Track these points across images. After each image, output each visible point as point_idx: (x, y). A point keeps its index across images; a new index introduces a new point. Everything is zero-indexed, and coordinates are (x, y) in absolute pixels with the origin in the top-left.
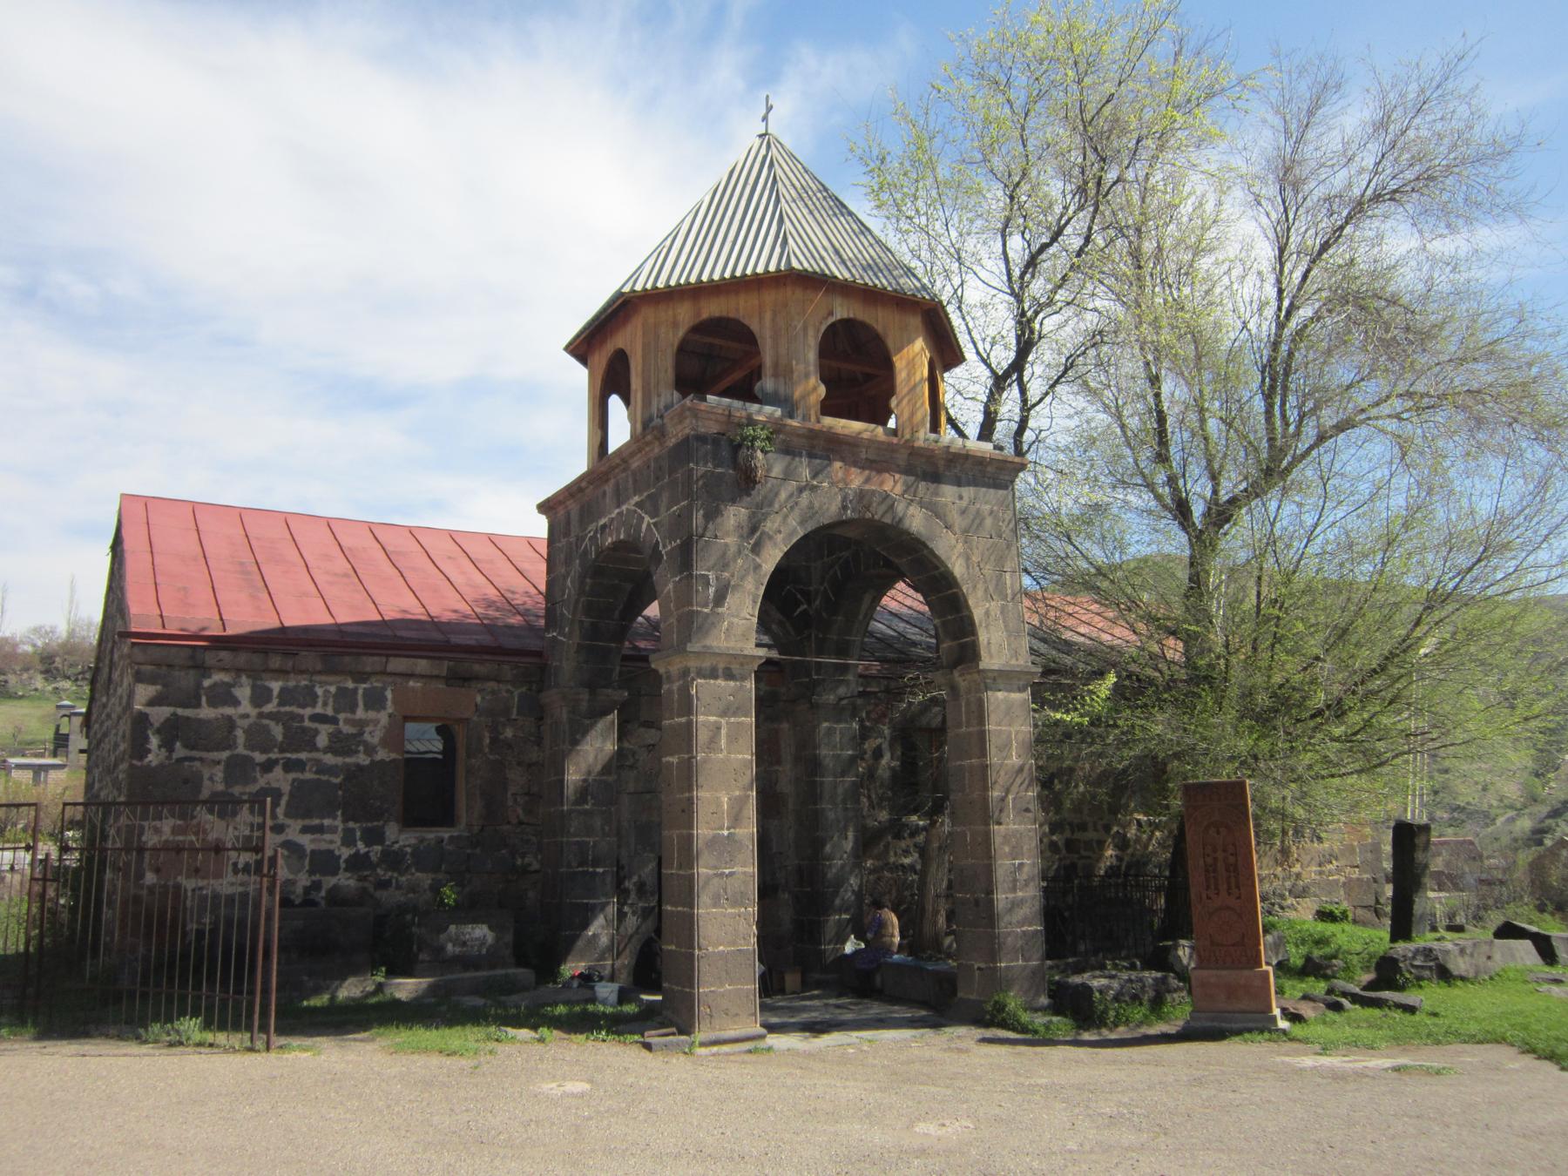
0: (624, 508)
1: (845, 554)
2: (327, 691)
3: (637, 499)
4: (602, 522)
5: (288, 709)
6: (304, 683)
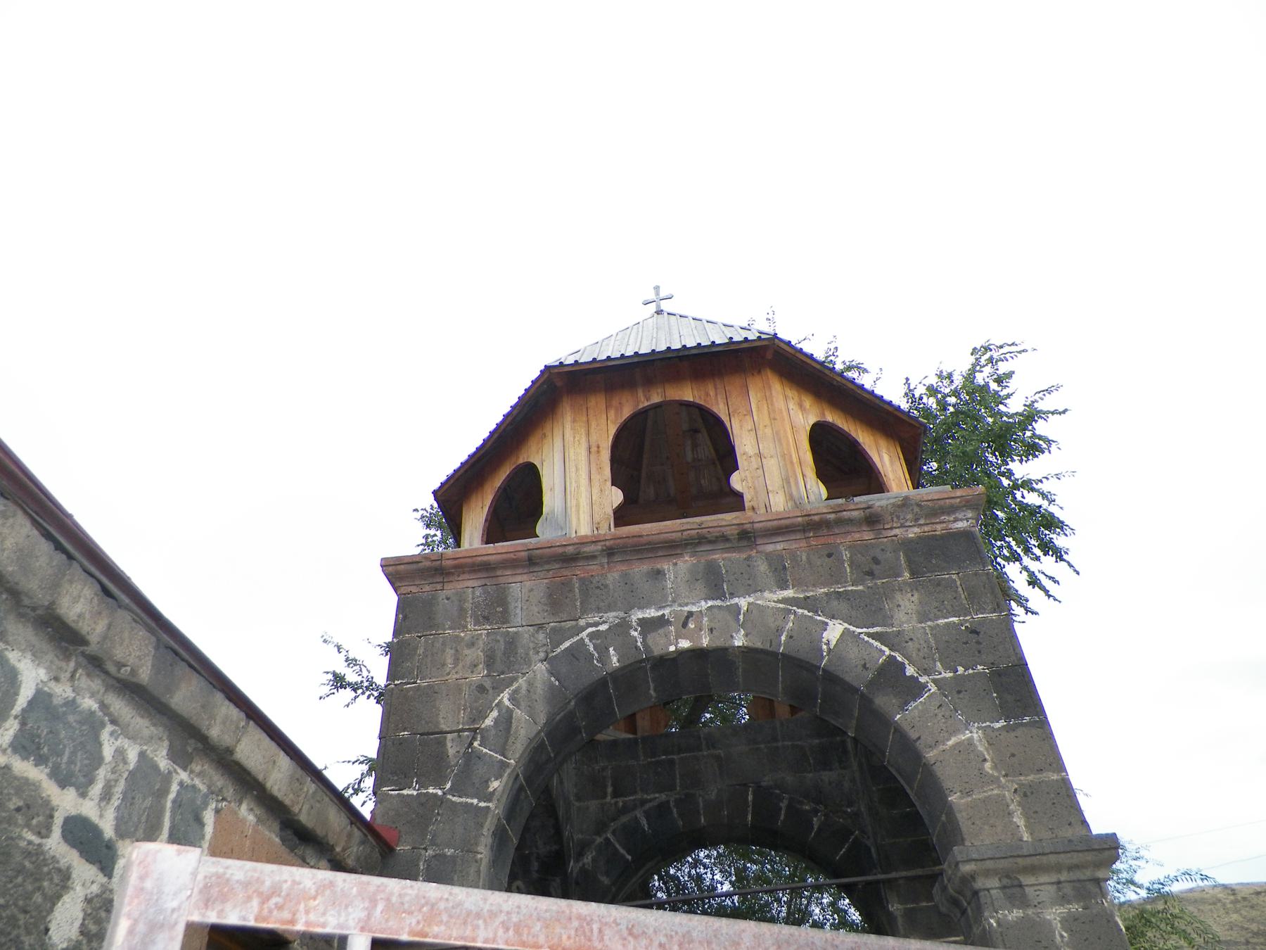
0: (743, 603)
1: (663, 797)
2: (120, 754)
3: (789, 593)
4: (652, 613)
5: (25, 768)
6: (89, 703)
